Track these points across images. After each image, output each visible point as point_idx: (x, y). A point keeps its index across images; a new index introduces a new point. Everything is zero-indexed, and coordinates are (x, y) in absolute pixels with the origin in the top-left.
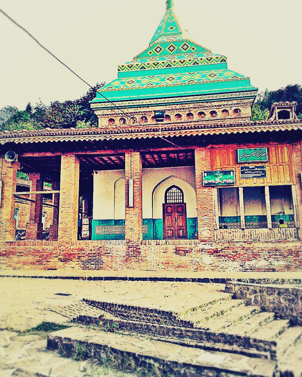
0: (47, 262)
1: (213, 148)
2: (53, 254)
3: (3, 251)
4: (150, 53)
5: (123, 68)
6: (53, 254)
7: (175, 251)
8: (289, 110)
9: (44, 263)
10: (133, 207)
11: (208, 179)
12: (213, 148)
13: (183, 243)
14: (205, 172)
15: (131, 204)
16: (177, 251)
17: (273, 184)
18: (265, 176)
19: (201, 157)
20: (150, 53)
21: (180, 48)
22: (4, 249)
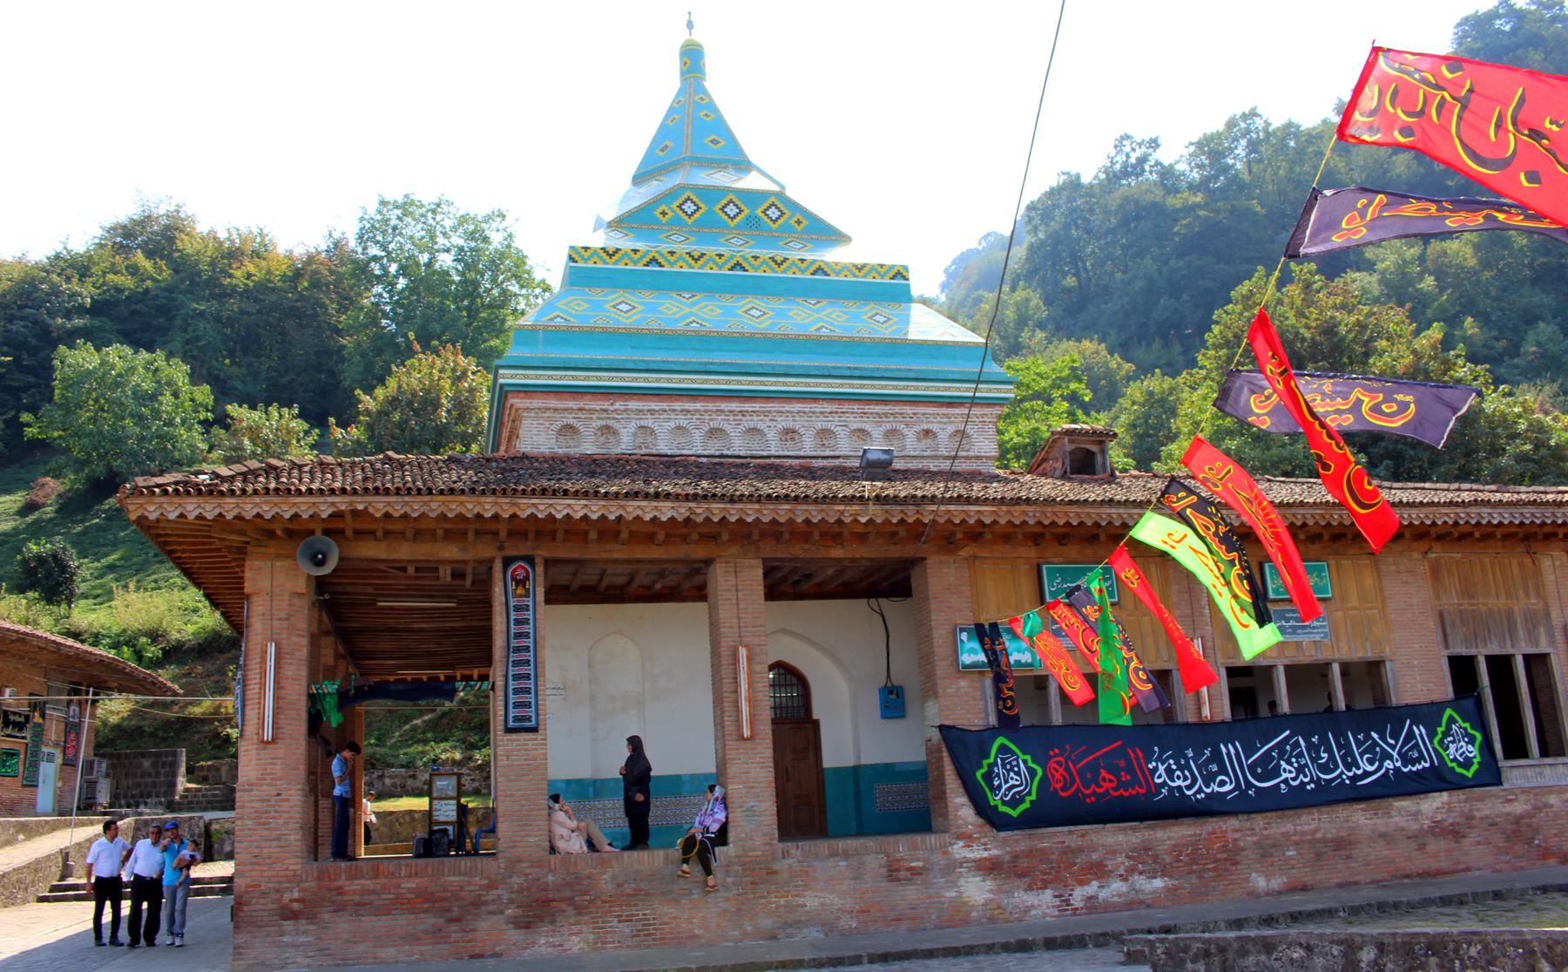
0: (463, 931)
1: (975, 557)
2: (486, 903)
3: (292, 901)
4: (664, 214)
5: (586, 255)
6: (486, 903)
7: (883, 870)
8: (1094, 448)
9: (454, 937)
10: (751, 738)
12: (975, 557)
13: (902, 846)
14: (962, 630)
15: (746, 733)
16: (893, 872)
19: (943, 580)
20: (664, 214)
21: (759, 212)
22: (296, 895)
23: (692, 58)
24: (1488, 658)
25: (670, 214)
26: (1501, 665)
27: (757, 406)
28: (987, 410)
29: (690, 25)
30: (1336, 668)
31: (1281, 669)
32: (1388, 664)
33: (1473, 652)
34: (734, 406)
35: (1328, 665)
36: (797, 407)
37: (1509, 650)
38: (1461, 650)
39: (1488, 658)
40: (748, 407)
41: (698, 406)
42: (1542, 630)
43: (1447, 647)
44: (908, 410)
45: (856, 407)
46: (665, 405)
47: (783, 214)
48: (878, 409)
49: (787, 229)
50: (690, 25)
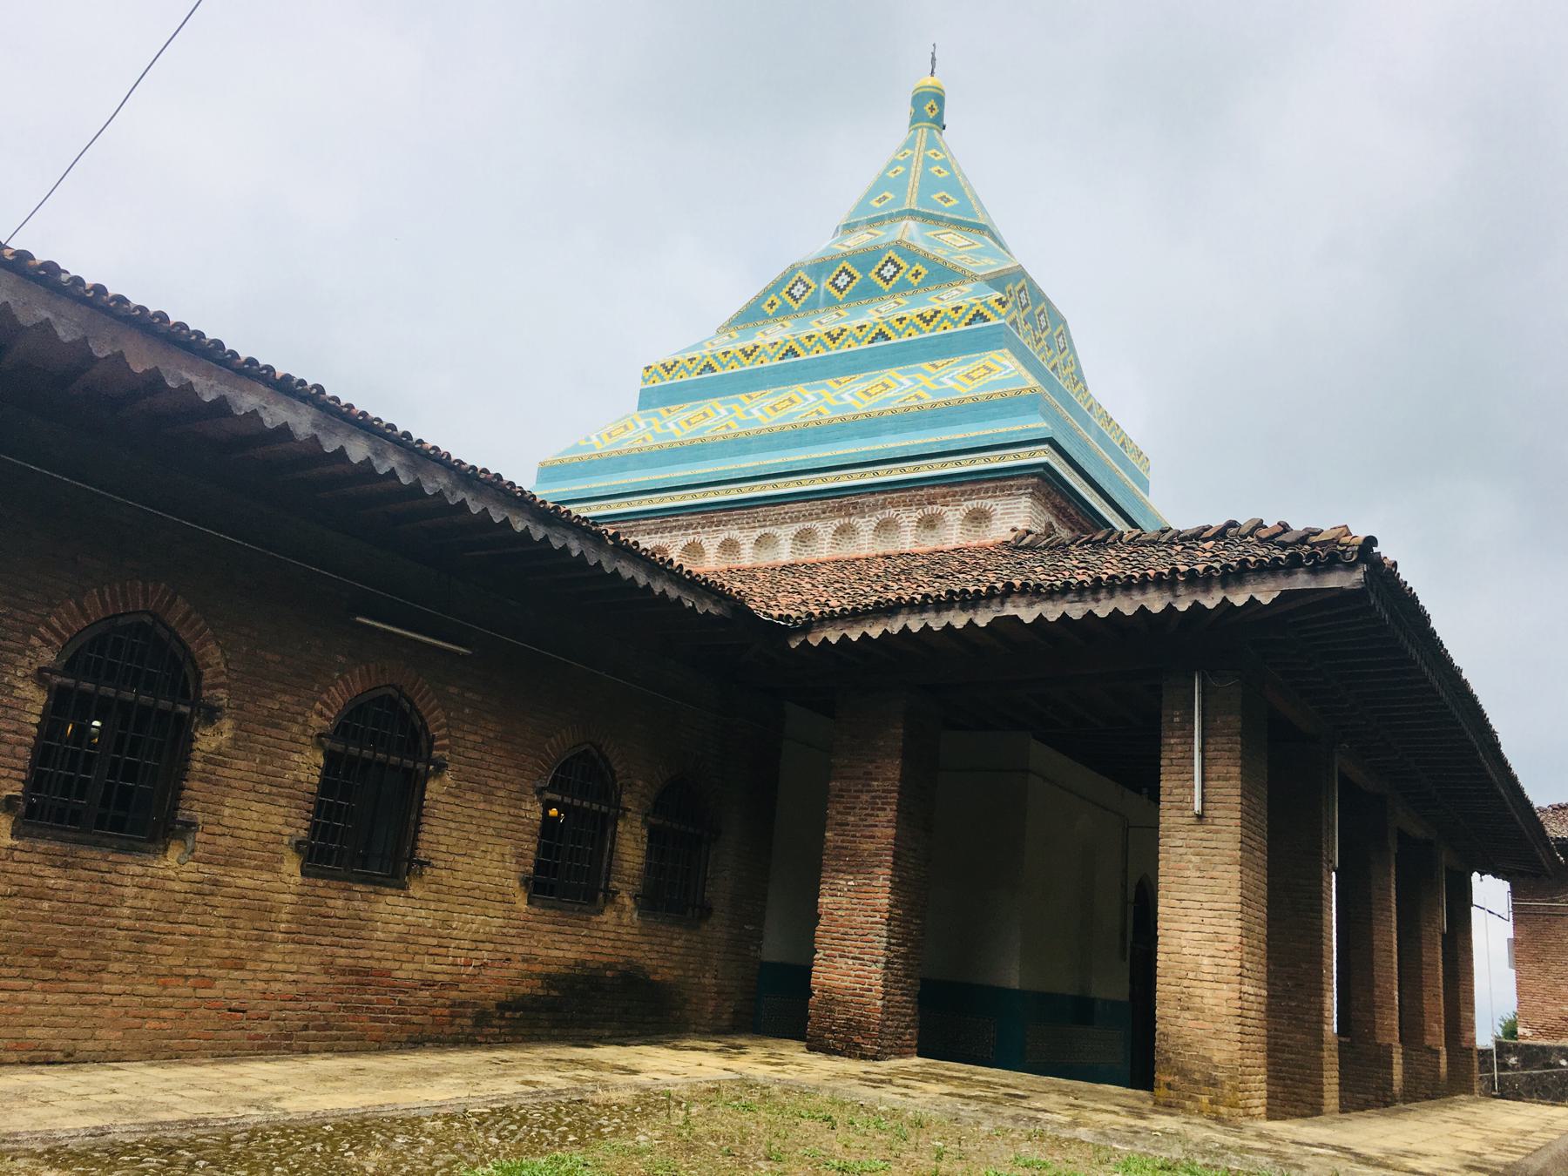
25: (779, 303)
47: (899, 268)
49: (904, 287)
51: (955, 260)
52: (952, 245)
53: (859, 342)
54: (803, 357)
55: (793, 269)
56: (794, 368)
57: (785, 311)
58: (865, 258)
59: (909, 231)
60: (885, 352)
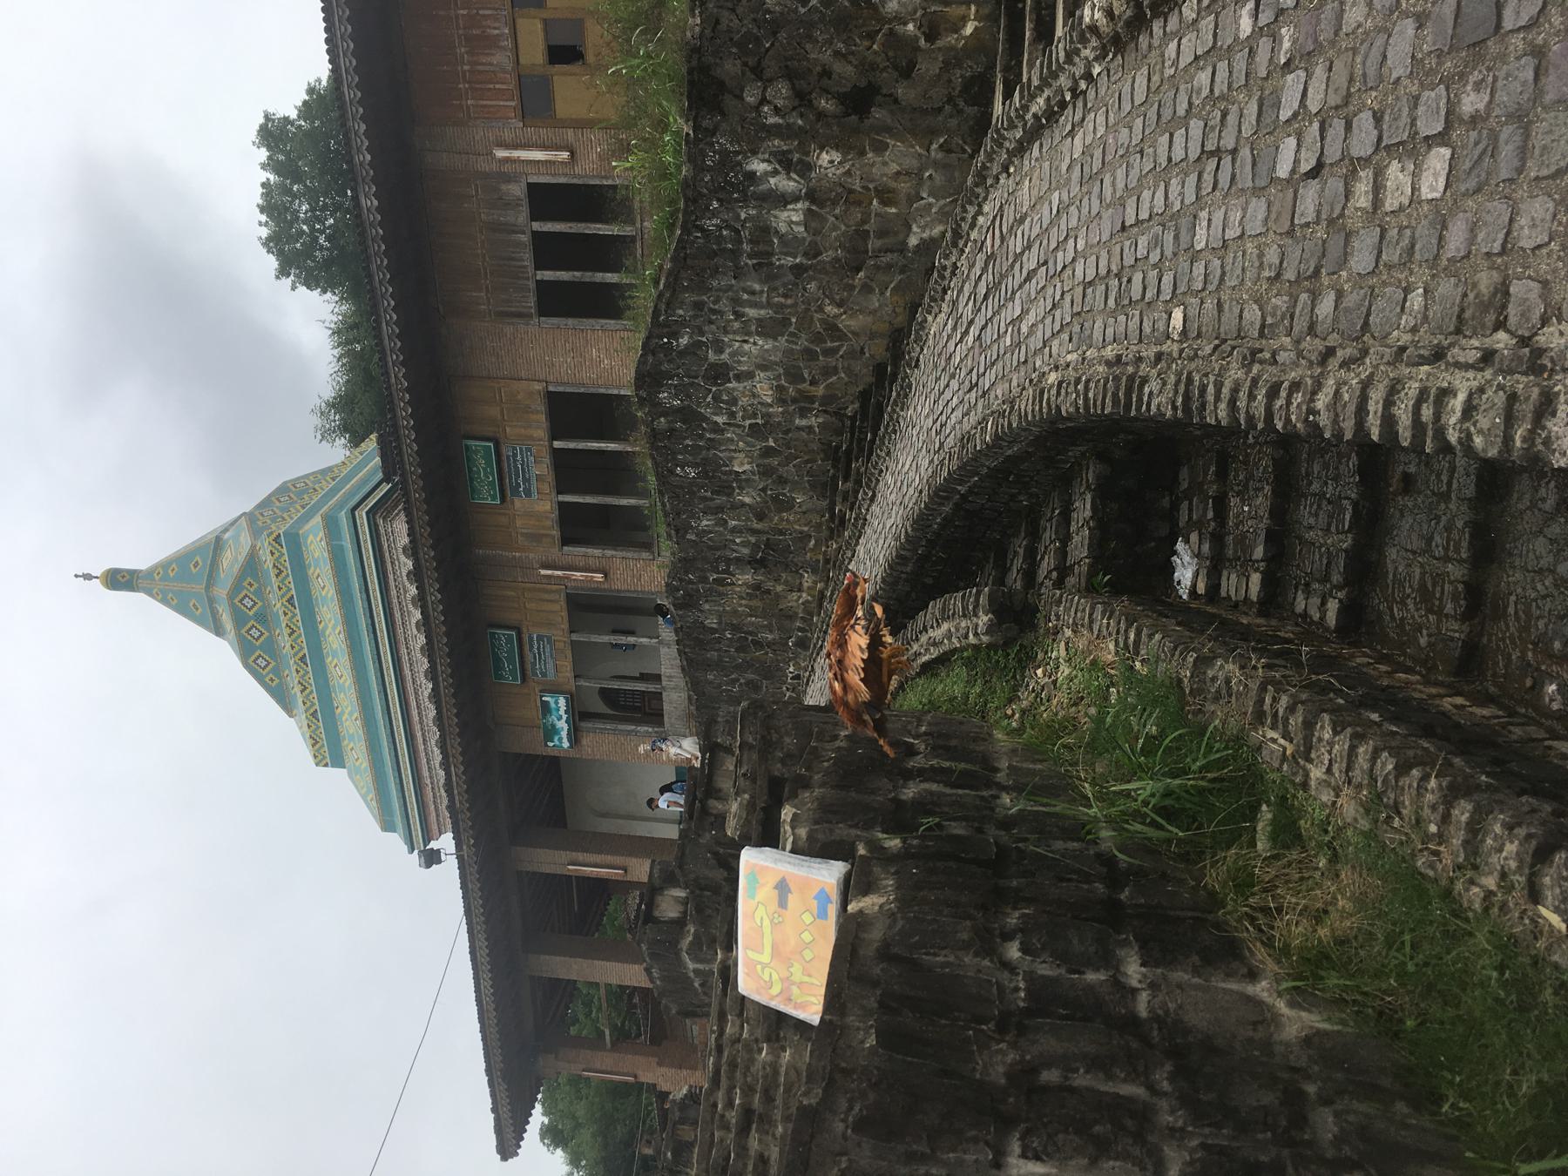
11: (560, 740)
17: (565, 626)
18: (549, 638)
23: (118, 580)
24: (537, 268)
26: (548, 250)
27: (412, 698)
28: (382, 531)
29: (88, 577)
30: (557, 444)
31: (562, 498)
32: (551, 389)
33: (532, 285)
34: (415, 713)
35: (556, 453)
36: (407, 672)
37: (525, 238)
38: (532, 302)
39: (537, 268)
40: (413, 704)
41: (419, 734)
42: (504, 187)
43: (530, 316)
44: (394, 592)
45: (400, 631)
46: (423, 754)
48: (398, 615)
49: (260, 593)
50: (88, 577)
51: (241, 559)
52: (231, 562)
53: (295, 615)
54: (306, 651)
55: (246, 666)
56: (315, 657)
57: (277, 671)
58: (239, 620)
59: (221, 591)
60: (304, 601)
